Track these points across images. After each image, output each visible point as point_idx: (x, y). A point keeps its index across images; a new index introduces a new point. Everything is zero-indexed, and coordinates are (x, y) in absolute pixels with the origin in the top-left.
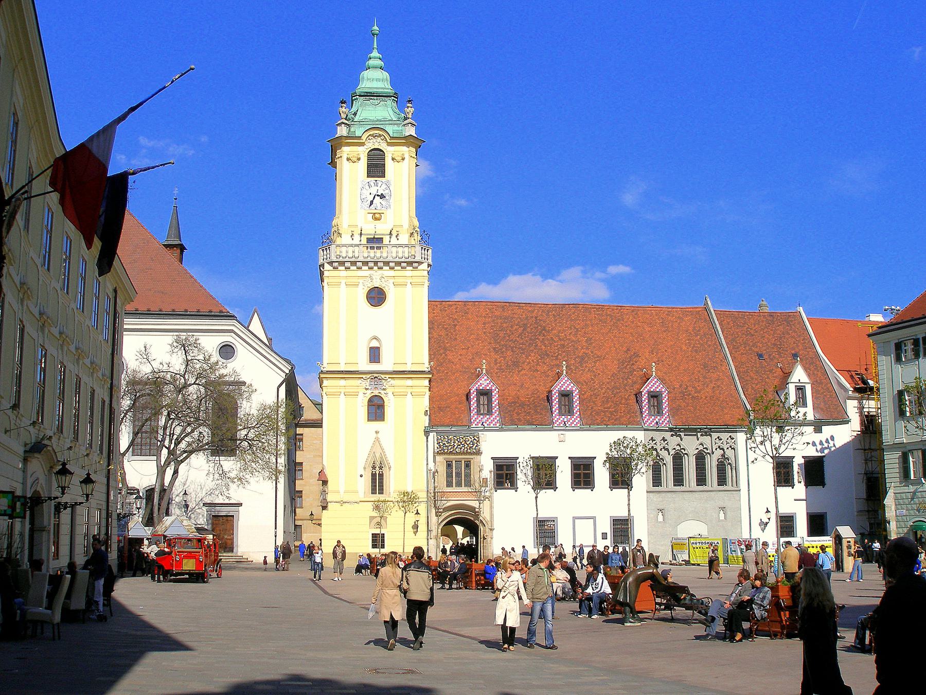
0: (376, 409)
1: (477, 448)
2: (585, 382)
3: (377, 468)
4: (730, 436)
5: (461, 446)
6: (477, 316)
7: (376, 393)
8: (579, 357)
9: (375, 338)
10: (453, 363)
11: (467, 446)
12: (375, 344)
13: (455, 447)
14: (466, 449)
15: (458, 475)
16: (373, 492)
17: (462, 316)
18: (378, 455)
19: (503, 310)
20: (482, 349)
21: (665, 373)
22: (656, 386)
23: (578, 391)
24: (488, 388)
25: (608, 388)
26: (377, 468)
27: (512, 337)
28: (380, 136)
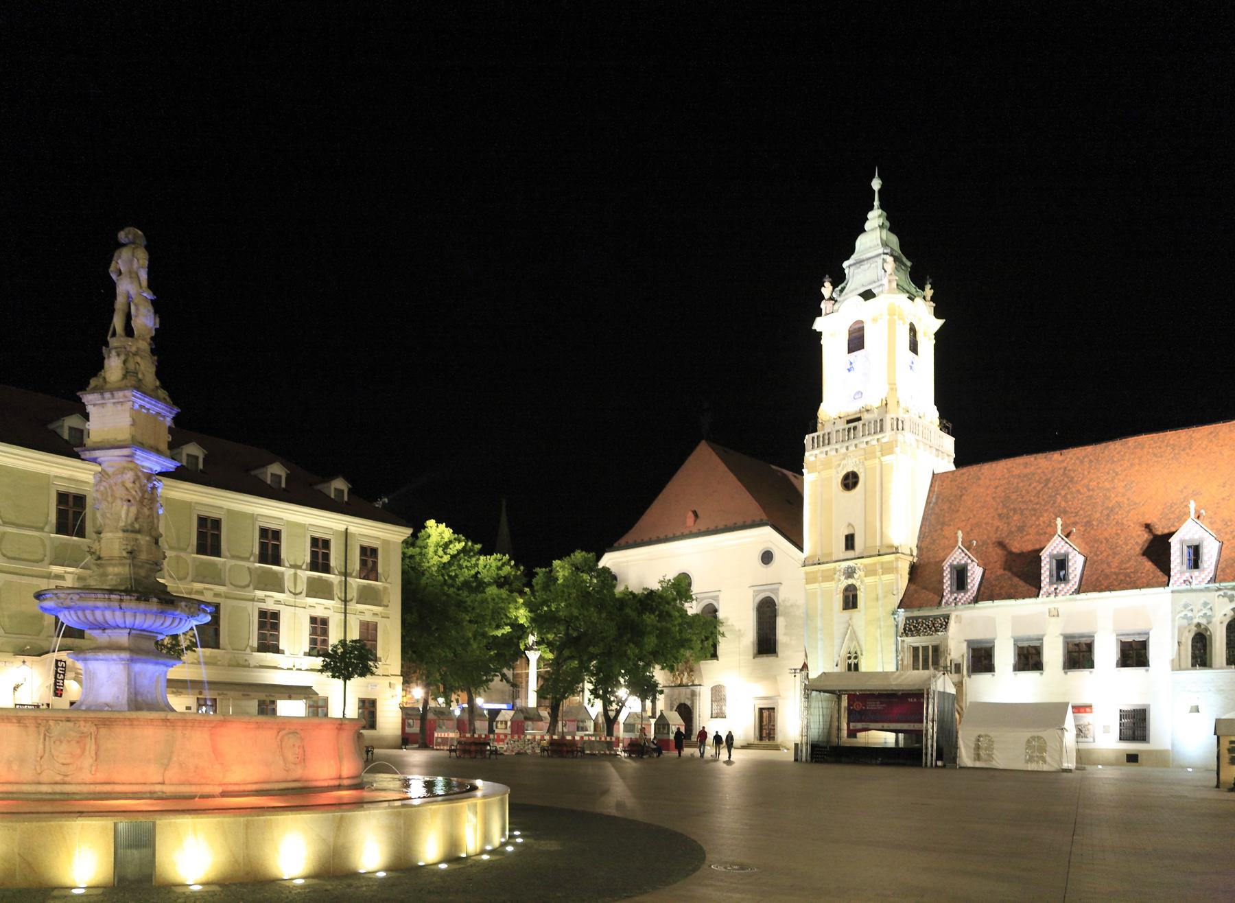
0: (850, 600)
2: (1106, 539)
6: (990, 480)
7: (850, 581)
8: (1107, 508)
10: (947, 538)
11: (933, 628)
17: (973, 483)
19: (1025, 467)
20: (985, 518)
25: (1137, 543)
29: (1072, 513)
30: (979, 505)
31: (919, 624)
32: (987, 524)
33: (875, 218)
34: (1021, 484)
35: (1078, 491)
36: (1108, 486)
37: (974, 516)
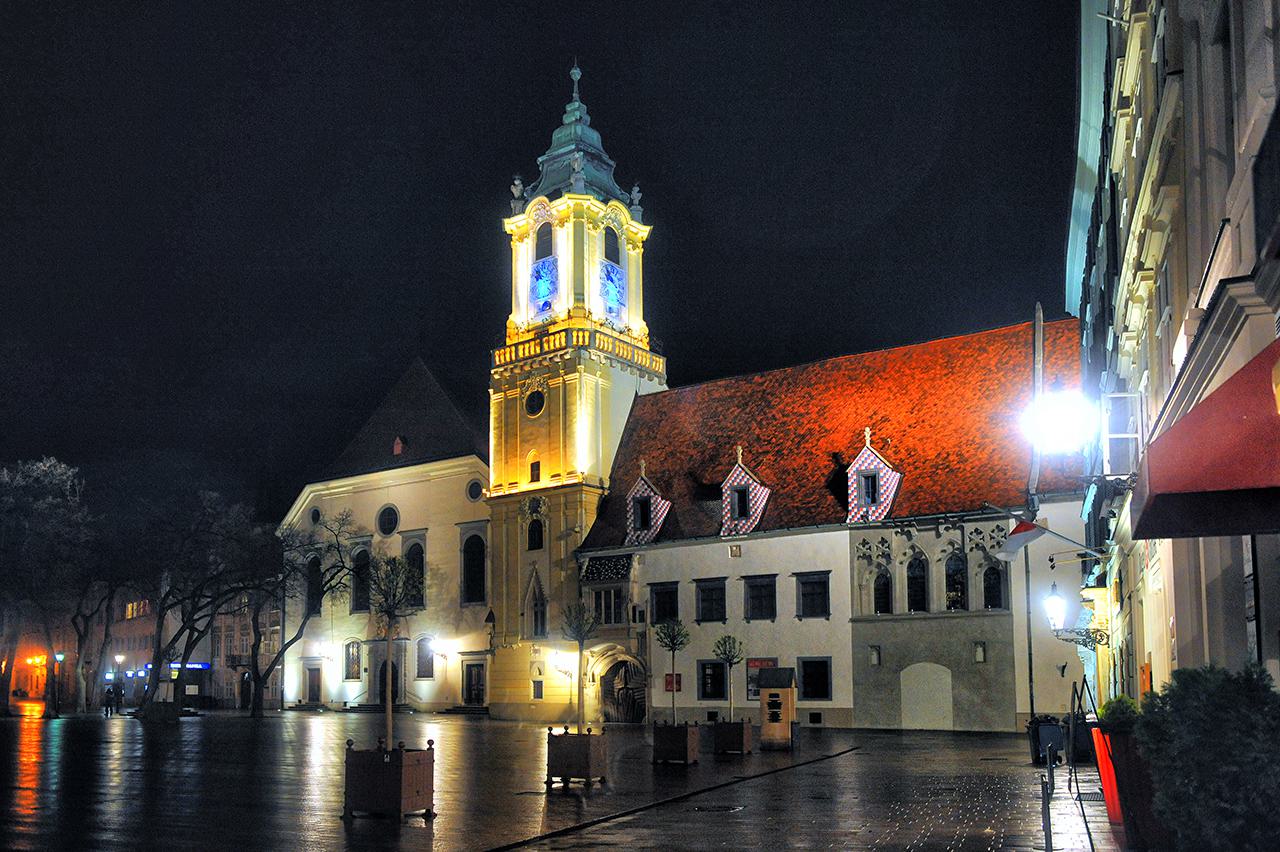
4: (998, 526)
8: (799, 435)
21: (920, 440)
22: (869, 461)
27: (723, 424)
29: (764, 441)
30: (676, 431)
32: (681, 452)
33: (575, 110)
34: (720, 409)
35: (774, 416)
36: (803, 411)
37: (670, 443)
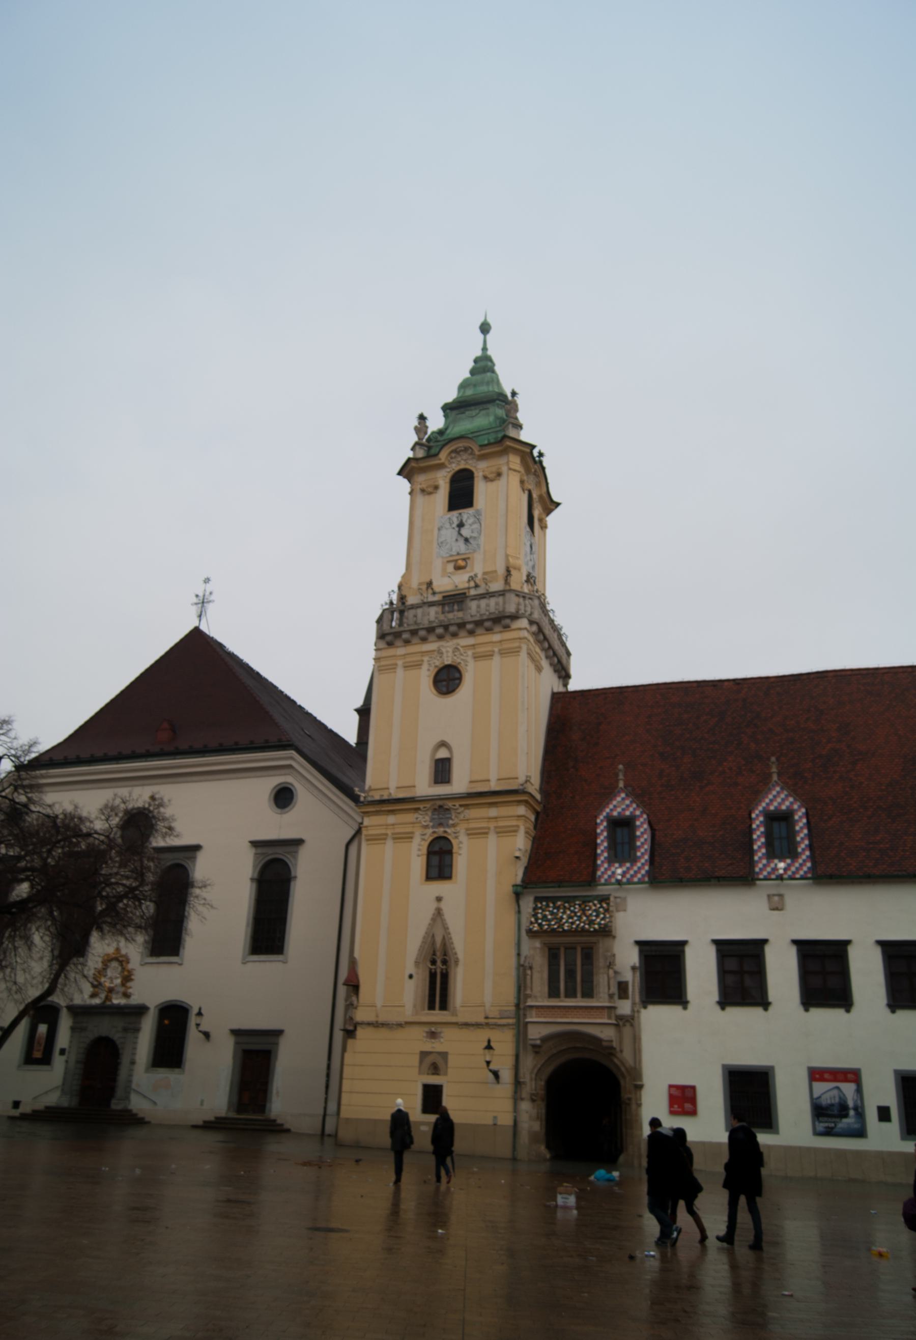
1: (603, 922)
3: (439, 963)
5: (575, 918)
7: (440, 831)
9: (443, 744)
11: (584, 918)
12: (442, 754)
13: (564, 921)
14: (582, 924)
15: (571, 974)
16: (431, 1007)
18: (439, 940)
23: (803, 810)
24: (628, 813)
26: (439, 963)
28: (466, 449)
31: (558, 908)
